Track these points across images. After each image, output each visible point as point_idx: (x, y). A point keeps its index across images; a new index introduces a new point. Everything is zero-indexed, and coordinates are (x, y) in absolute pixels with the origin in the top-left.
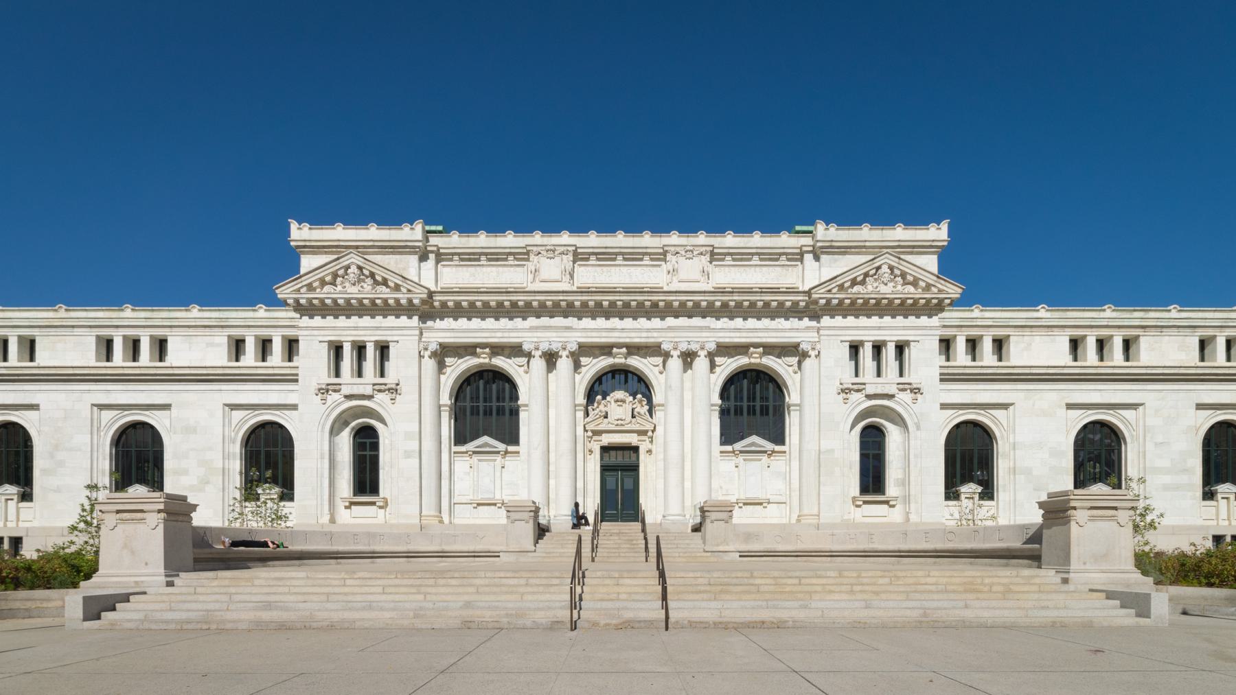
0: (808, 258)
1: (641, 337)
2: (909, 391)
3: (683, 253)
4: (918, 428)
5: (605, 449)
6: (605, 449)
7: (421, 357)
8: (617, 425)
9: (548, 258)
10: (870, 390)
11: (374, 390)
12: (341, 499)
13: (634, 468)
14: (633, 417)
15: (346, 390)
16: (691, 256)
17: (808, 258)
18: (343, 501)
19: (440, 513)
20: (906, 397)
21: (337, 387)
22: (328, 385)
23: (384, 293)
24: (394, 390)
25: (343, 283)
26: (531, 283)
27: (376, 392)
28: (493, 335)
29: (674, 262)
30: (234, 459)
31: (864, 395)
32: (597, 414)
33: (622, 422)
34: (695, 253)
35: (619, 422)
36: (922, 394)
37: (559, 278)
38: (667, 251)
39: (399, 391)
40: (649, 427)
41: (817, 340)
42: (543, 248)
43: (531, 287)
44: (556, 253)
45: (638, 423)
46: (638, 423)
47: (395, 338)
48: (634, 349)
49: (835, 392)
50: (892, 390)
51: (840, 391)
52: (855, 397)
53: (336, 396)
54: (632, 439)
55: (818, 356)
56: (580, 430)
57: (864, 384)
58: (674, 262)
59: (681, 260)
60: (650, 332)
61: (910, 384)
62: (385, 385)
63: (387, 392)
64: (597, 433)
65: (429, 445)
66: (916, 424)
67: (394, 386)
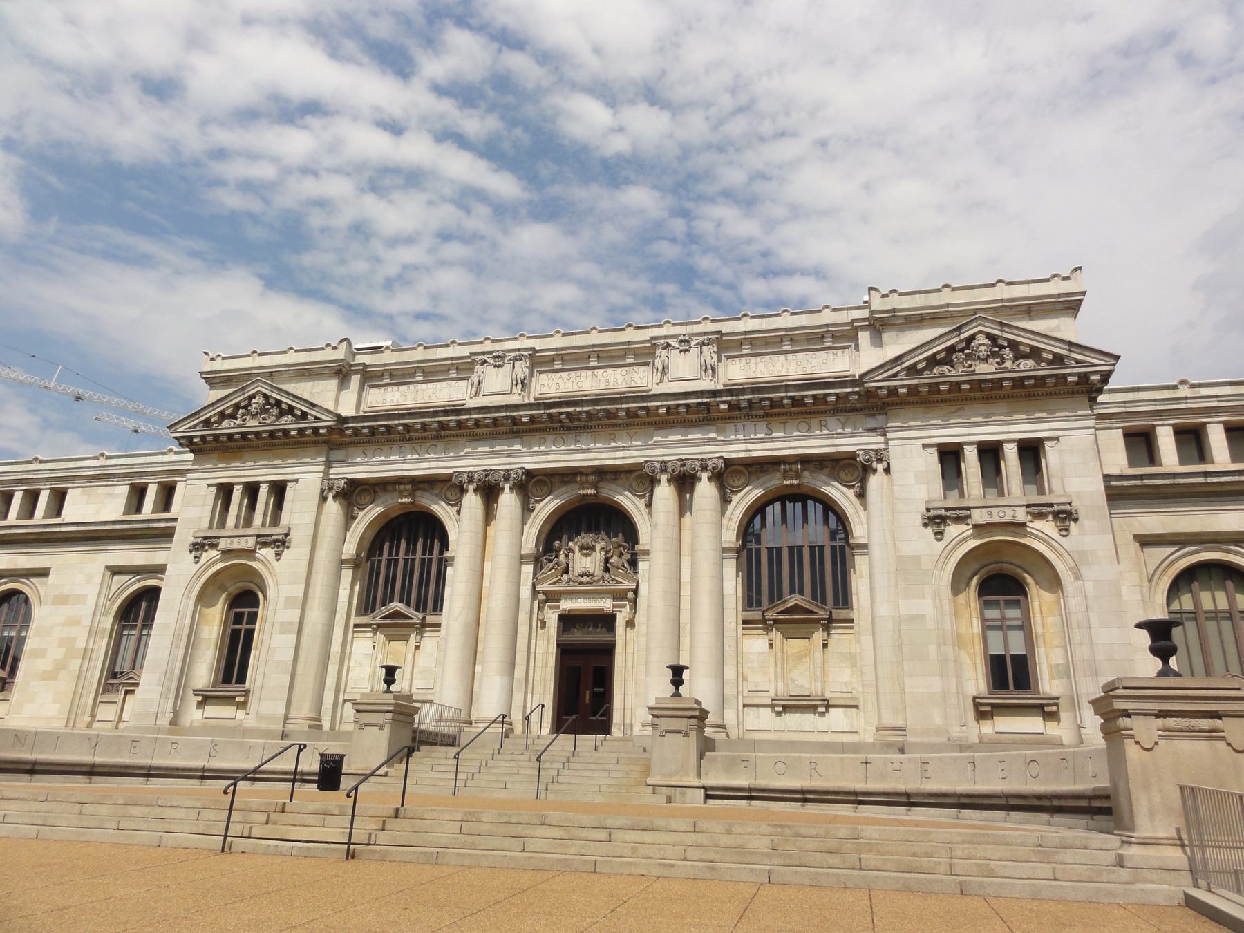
0: (864, 337)
1: (615, 458)
2: (1050, 517)
3: (677, 345)
4: (1078, 576)
5: (567, 621)
6: (567, 621)
7: (324, 499)
8: (581, 583)
9: (495, 366)
10: (979, 516)
11: (257, 543)
12: (194, 691)
13: (608, 651)
14: (607, 570)
15: (223, 544)
16: (687, 348)
17: (864, 337)
18: (195, 695)
19: (320, 715)
20: (1047, 527)
21: (215, 541)
22: (205, 538)
23: (288, 423)
24: (280, 544)
25: (244, 414)
26: (471, 398)
27: (258, 546)
28: (417, 466)
29: (663, 357)
30: (103, 637)
31: (971, 526)
32: (553, 568)
33: (588, 579)
34: (693, 343)
35: (585, 579)
36: (1076, 520)
37: (508, 389)
38: (655, 344)
39: (287, 544)
40: (627, 585)
41: (883, 446)
42: (491, 356)
43: (471, 403)
44: (506, 359)
45: (613, 580)
46: (613, 580)
47: (295, 477)
48: (604, 474)
49: (919, 521)
50: (1021, 515)
51: (926, 521)
52: (953, 530)
53: (213, 553)
54: (607, 604)
55: (887, 470)
56: (526, 592)
57: (969, 508)
58: (663, 357)
59: (674, 353)
60: (628, 450)
61: (1051, 505)
62: (271, 535)
63: (272, 546)
64: (552, 597)
65: (316, 615)
66: (1071, 569)
67: (280, 537)
